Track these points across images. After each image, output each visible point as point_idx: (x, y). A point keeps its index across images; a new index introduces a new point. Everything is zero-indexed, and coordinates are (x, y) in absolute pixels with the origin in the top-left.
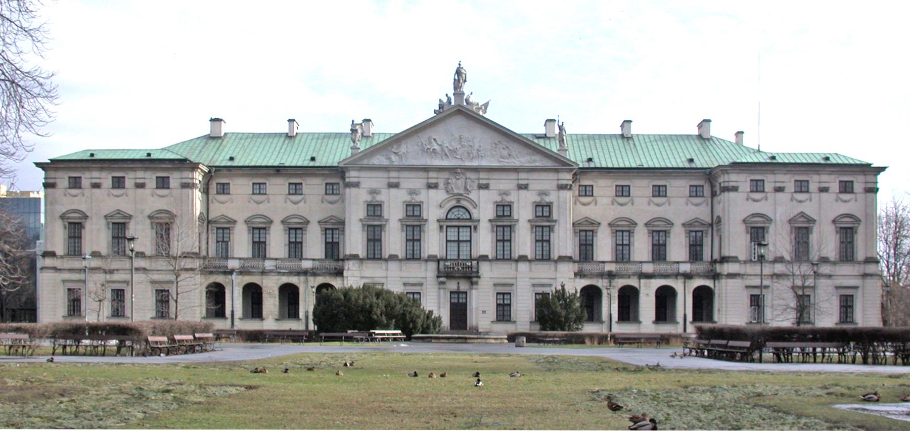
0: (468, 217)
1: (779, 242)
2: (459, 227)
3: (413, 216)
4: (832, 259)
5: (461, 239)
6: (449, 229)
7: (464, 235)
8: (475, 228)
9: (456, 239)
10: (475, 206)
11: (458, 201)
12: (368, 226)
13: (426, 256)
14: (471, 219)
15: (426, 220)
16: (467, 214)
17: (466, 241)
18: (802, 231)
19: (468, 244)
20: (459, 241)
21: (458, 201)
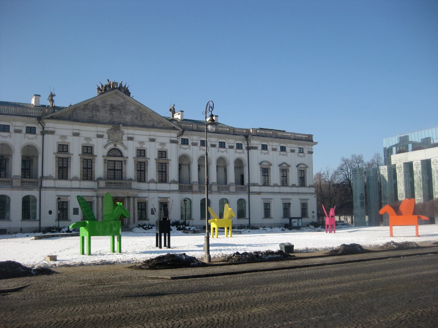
0: (120, 155)
1: (275, 176)
2: (115, 161)
3: (87, 153)
4: (260, 184)
5: (116, 168)
6: (109, 162)
7: (118, 167)
8: (125, 161)
9: (113, 168)
10: (126, 148)
11: (115, 145)
12: (59, 158)
13: (71, 177)
14: (122, 156)
15: (96, 156)
16: (119, 153)
17: (119, 170)
18: (284, 171)
19: (120, 172)
20: (115, 170)
21: (115, 145)
